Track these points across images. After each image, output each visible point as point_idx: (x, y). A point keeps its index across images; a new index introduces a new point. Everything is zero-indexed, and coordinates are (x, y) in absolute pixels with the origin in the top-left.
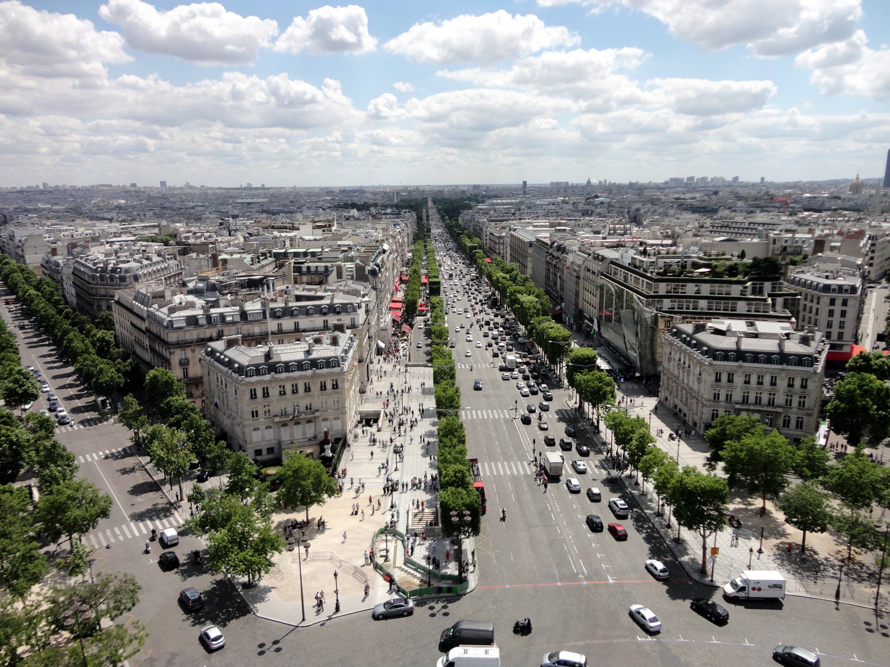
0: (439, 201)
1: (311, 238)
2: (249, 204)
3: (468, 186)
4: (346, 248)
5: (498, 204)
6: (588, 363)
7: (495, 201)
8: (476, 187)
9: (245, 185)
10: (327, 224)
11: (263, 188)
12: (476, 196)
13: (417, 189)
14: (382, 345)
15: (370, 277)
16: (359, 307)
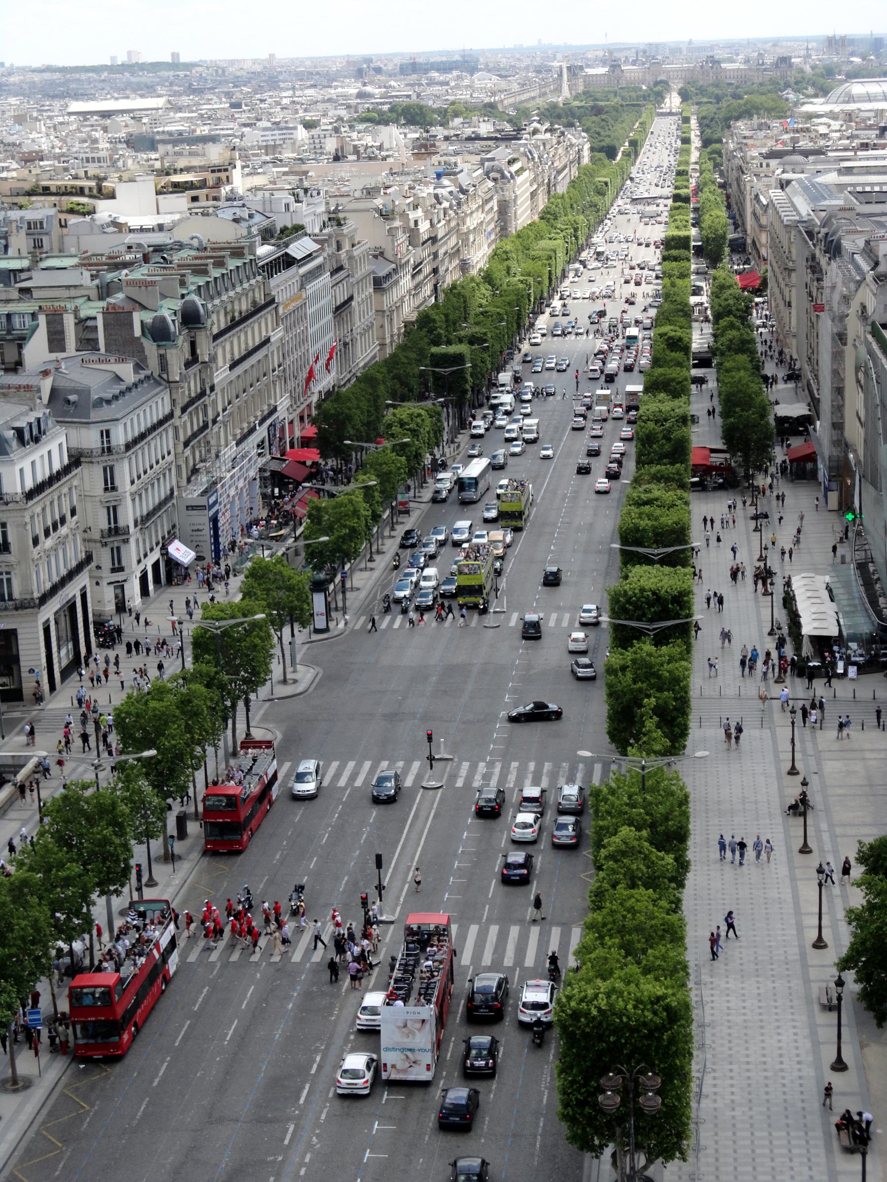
0: (702, 91)
1: (150, 221)
2: (106, 115)
3: (808, 41)
4: (128, 257)
5: (869, 98)
6: (665, 614)
7: (857, 88)
8: (834, 43)
9: (122, 59)
10: (211, 178)
11: (175, 65)
12: (829, 72)
13: (649, 56)
14: (182, 553)
15: (150, 348)
16: (30, 437)
